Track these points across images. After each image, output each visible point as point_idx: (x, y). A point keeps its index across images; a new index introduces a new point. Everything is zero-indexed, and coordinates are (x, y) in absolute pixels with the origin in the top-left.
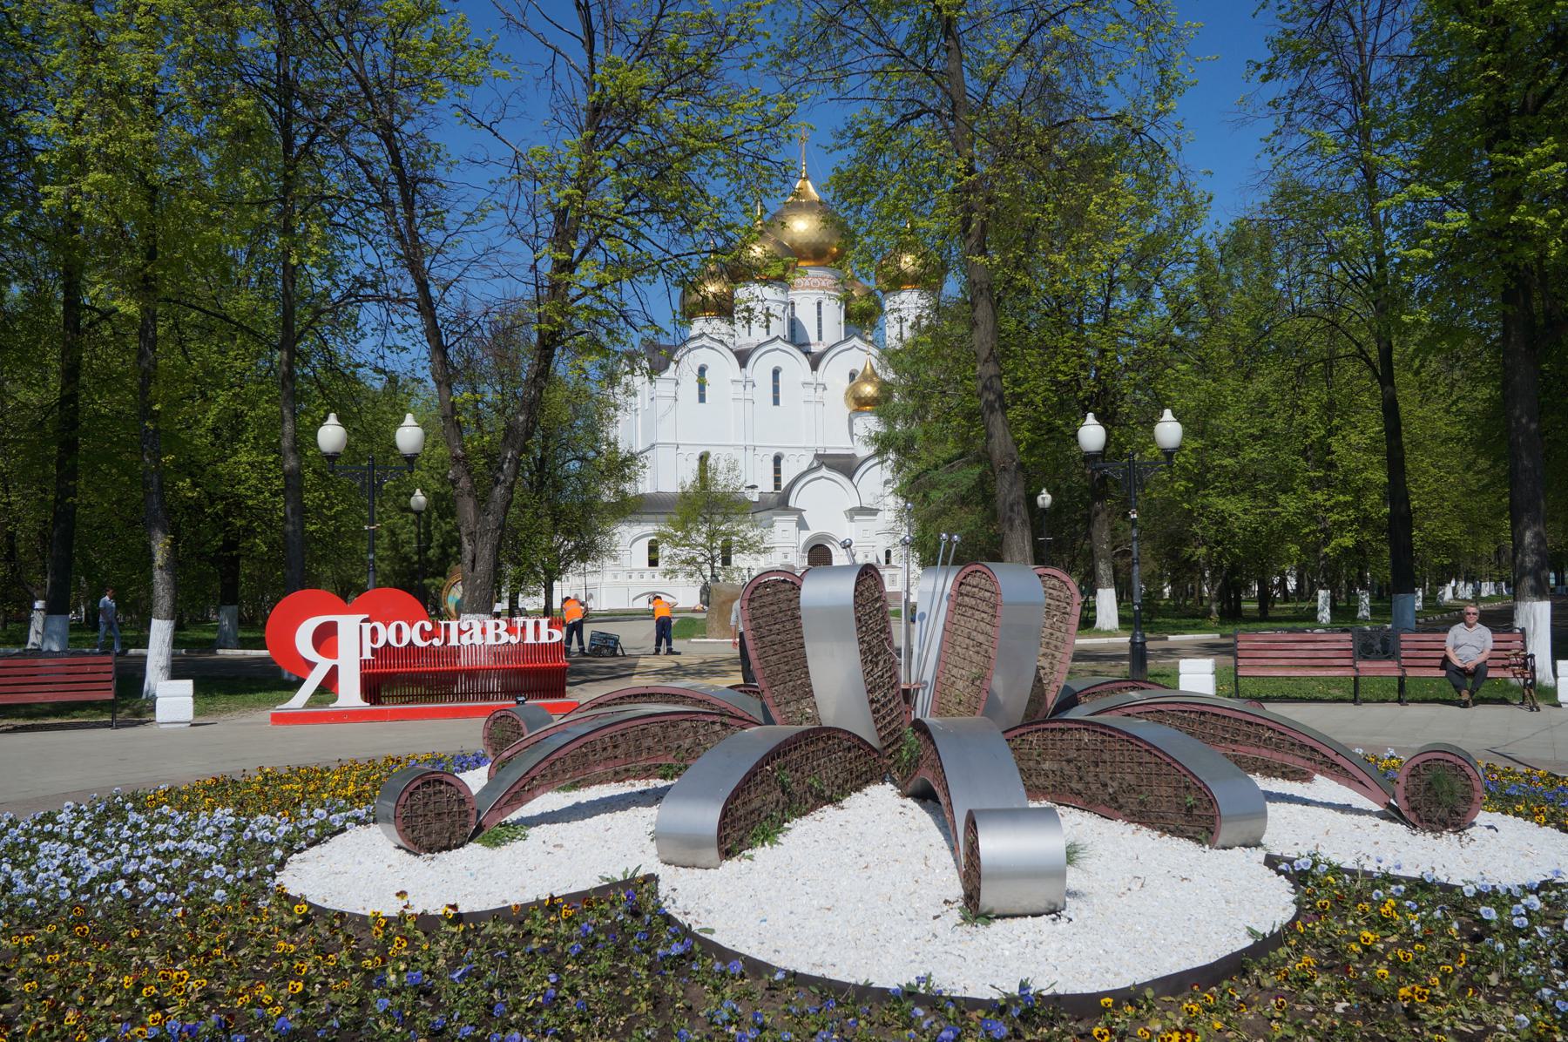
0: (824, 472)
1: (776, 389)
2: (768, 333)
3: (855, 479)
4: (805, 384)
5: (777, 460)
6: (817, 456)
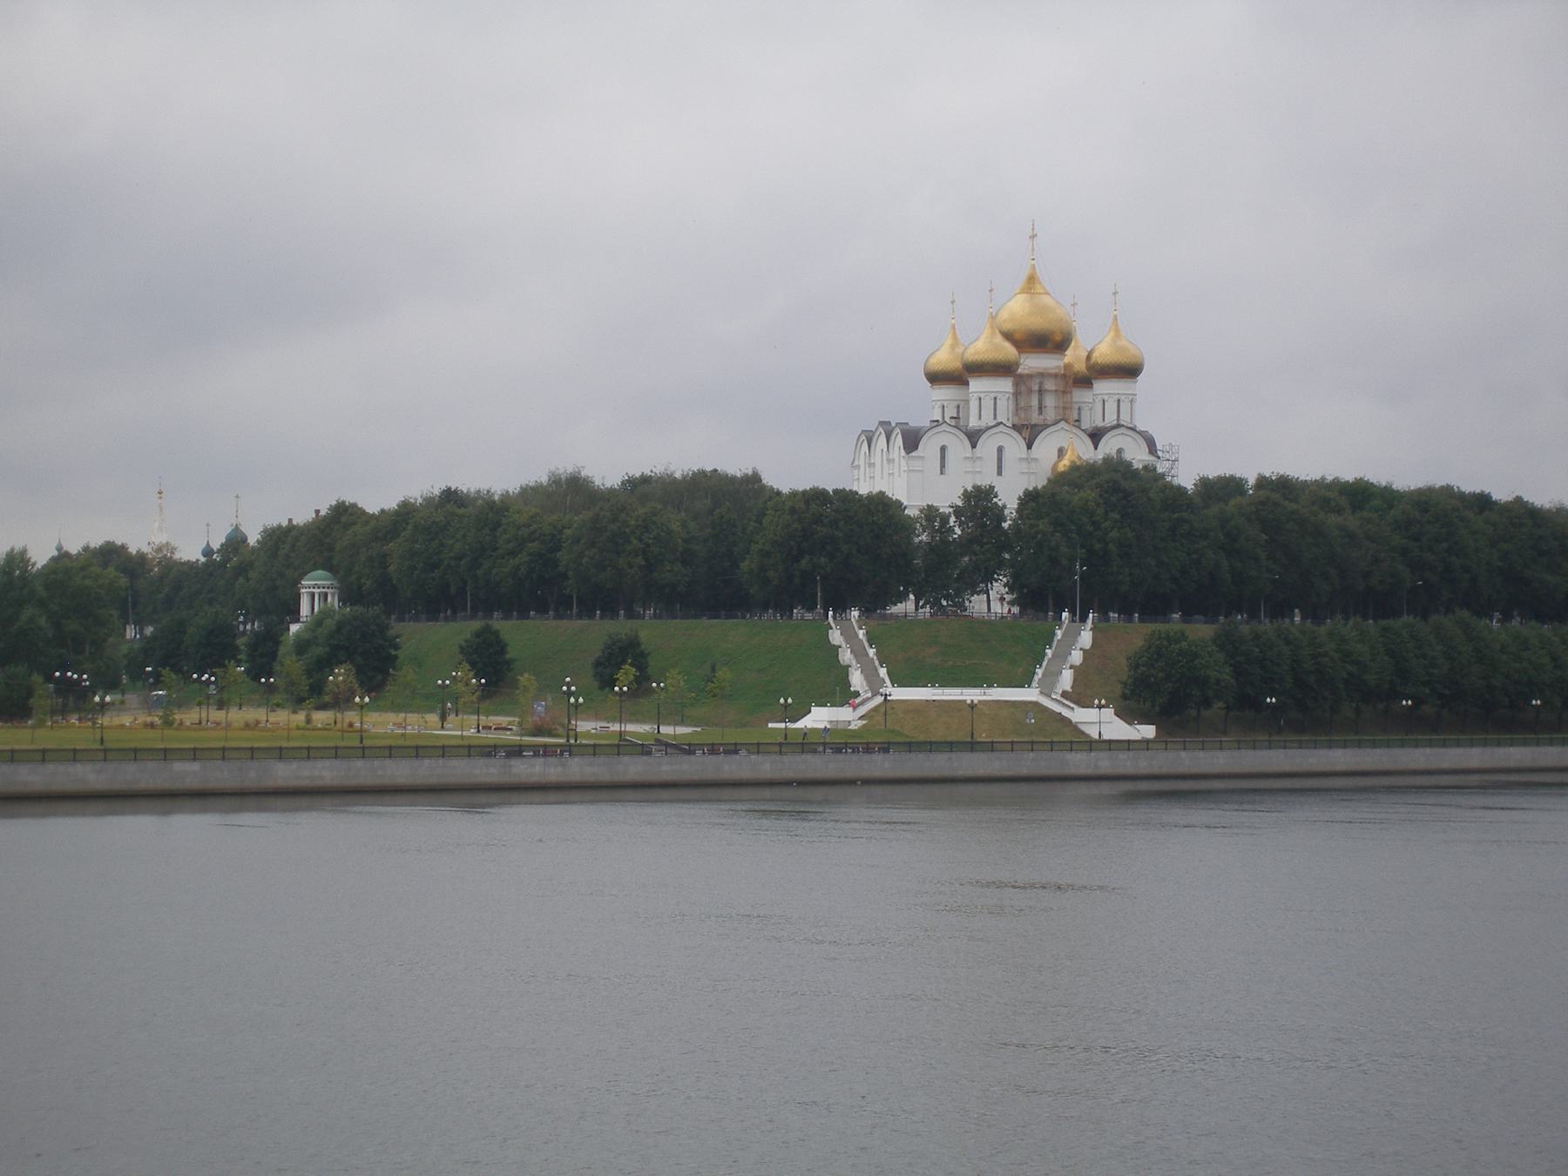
2: (995, 418)
4: (1021, 459)
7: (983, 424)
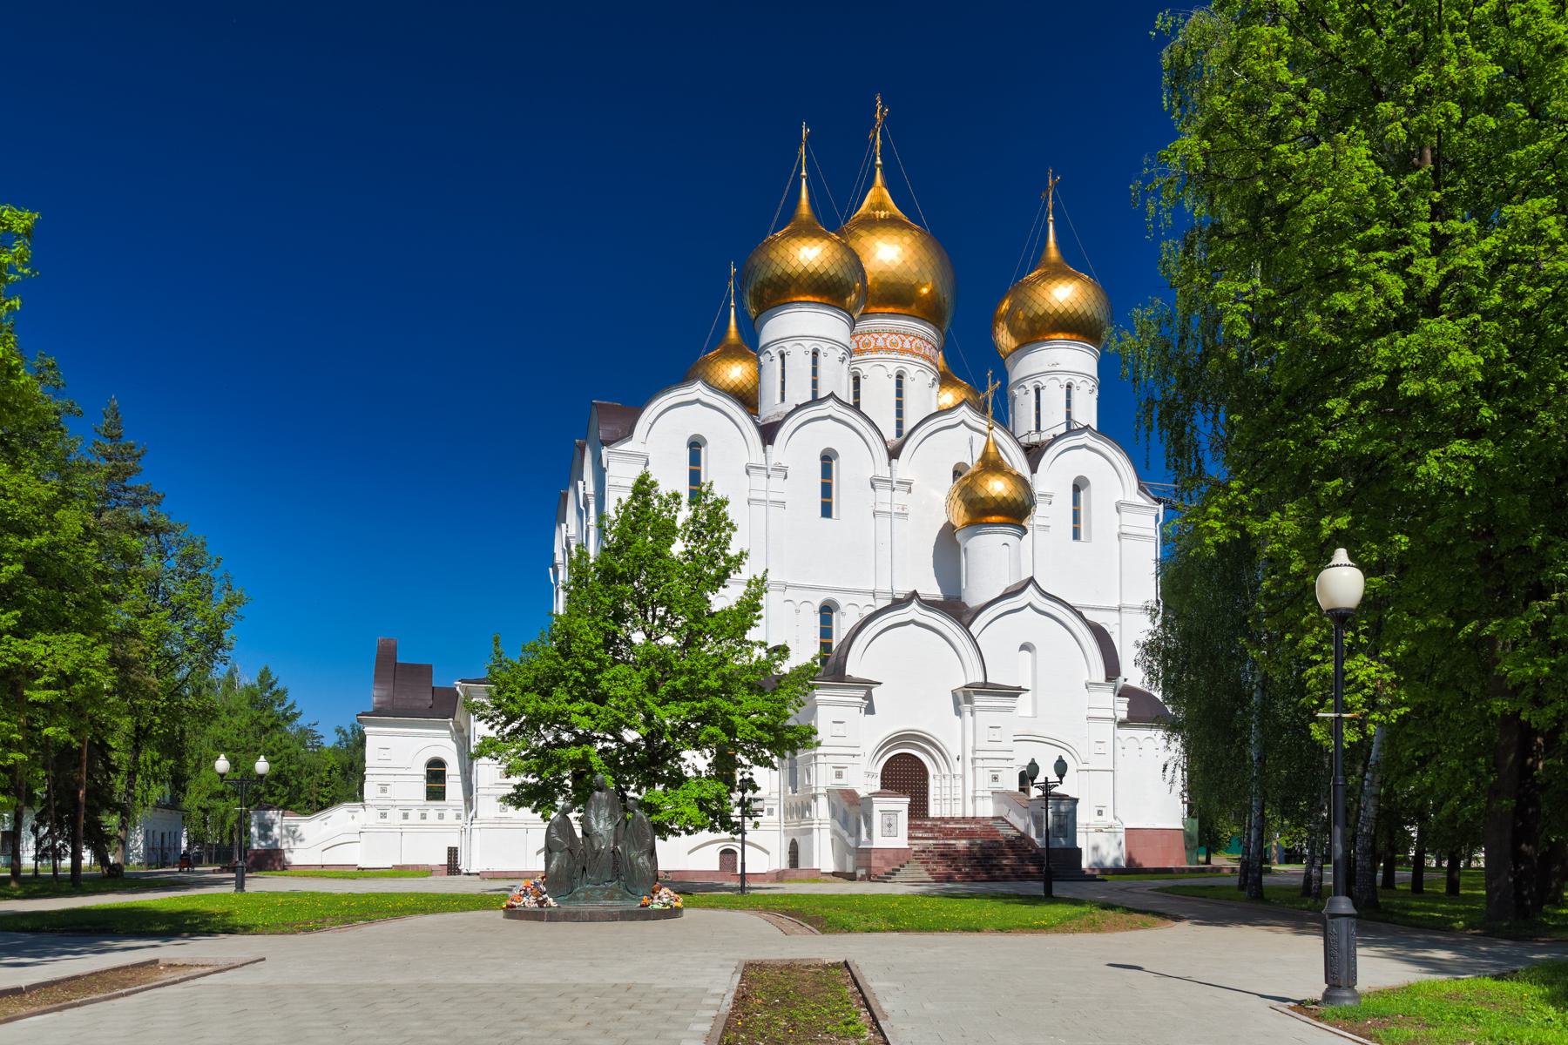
1: (827, 490)
2: (815, 393)
3: (975, 628)
5: (827, 610)
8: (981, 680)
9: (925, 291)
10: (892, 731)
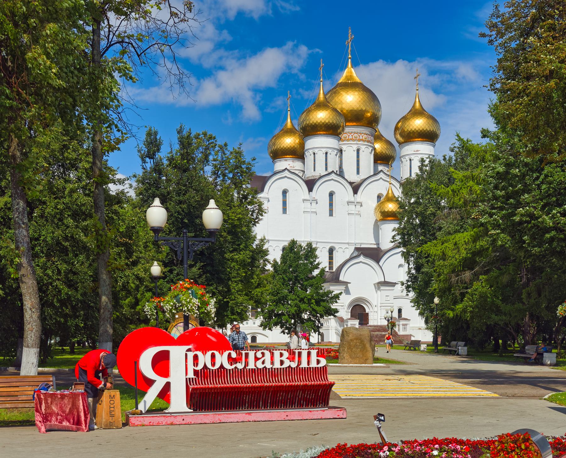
0: (362, 258)
2: (326, 169)
3: (381, 263)
4: (349, 203)
6: (357, 249)
7: (317, 174)
8: (383, 280)
9: (369, 115)
10: (354, 298)
